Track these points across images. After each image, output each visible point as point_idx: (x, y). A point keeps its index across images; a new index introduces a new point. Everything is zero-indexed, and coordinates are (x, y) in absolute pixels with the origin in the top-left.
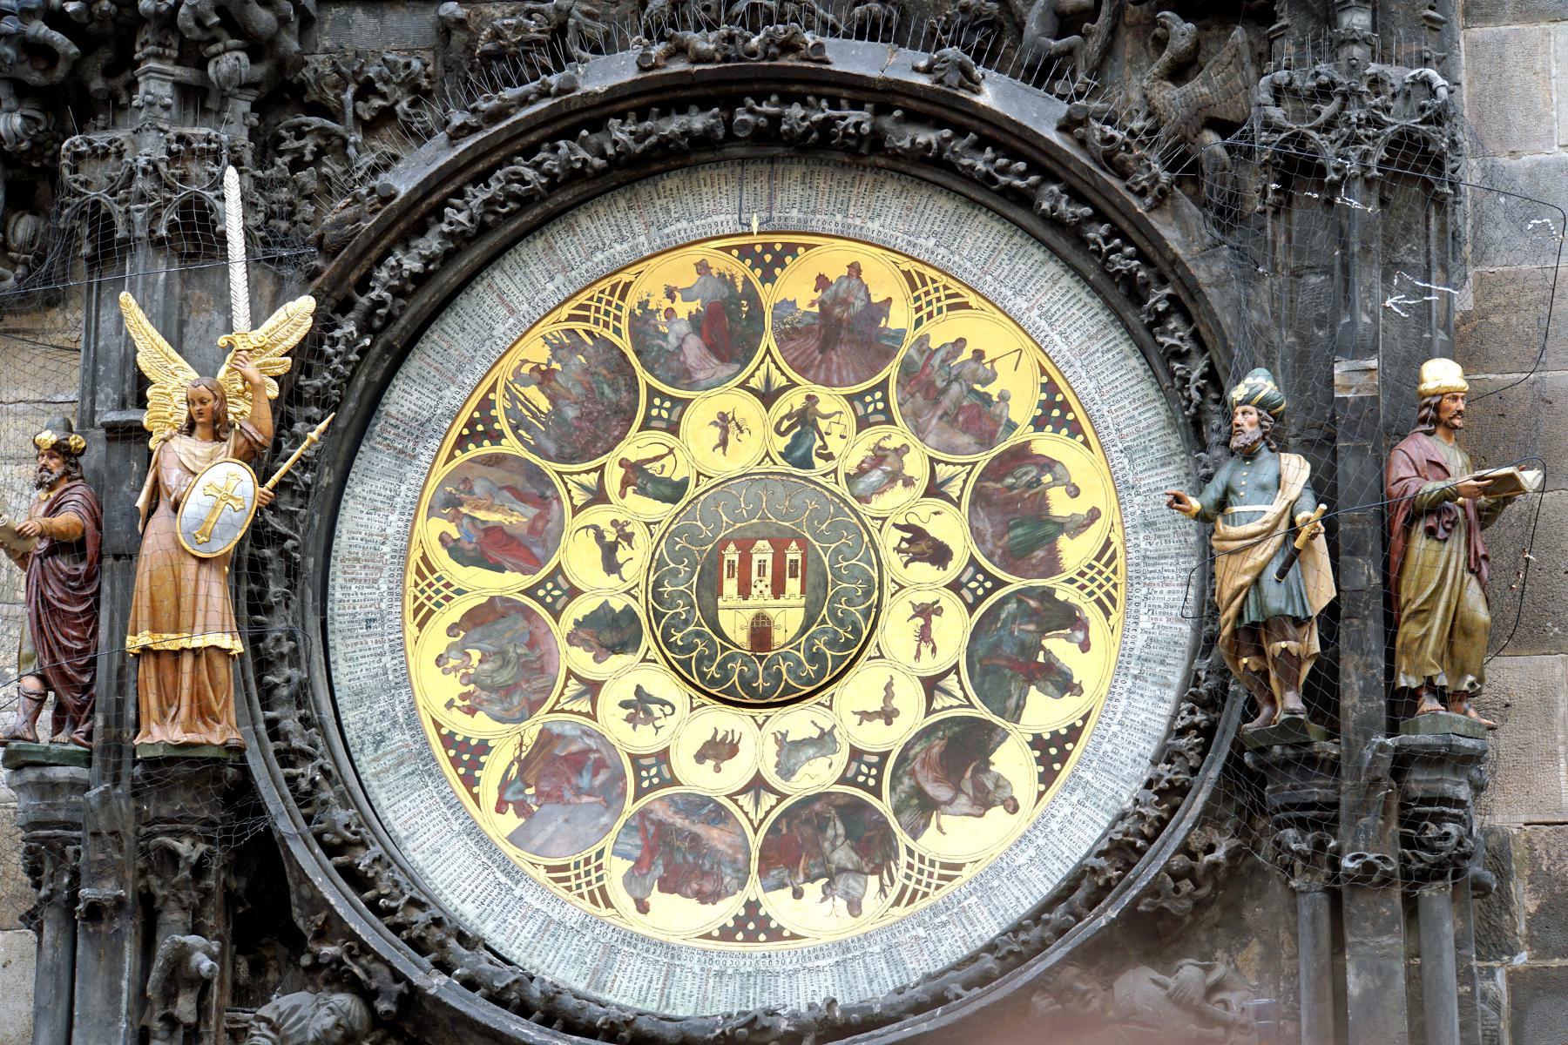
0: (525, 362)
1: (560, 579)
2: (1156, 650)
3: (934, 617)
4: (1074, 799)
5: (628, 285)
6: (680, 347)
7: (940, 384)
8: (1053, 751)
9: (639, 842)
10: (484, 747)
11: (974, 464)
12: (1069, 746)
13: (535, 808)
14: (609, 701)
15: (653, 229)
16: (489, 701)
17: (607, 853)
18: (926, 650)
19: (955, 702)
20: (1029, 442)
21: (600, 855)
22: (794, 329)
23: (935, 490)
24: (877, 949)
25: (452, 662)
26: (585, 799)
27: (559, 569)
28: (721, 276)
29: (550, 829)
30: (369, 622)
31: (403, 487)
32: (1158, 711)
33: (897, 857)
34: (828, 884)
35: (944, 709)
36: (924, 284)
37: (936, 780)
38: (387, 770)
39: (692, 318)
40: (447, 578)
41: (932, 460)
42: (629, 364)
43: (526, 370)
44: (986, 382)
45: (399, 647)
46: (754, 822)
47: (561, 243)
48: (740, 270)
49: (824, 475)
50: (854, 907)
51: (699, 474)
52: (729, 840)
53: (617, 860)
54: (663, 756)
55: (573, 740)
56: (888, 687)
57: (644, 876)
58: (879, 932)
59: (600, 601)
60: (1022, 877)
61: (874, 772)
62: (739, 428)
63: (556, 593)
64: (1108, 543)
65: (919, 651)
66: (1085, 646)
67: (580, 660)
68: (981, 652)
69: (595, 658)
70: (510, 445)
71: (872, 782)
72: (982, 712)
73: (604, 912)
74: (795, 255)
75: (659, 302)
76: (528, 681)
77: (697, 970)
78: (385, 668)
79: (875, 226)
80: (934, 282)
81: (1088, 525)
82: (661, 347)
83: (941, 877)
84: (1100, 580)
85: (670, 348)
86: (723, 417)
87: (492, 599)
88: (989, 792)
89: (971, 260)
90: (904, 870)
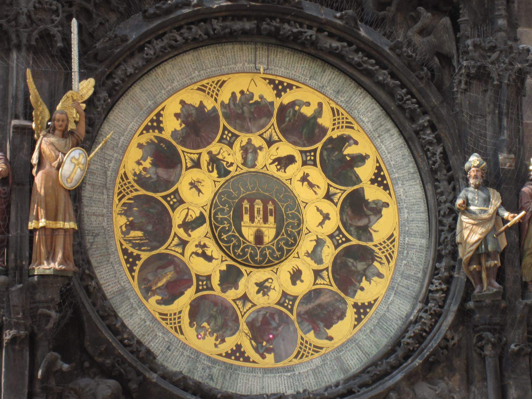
0: (121, 227)
1: (201, 278)
2: (376, 124)
3: (308, 178)
5: (125, 173)
6: (158, 176)
7: (240, 112)
9: (307, 324)
10: (239, 347)
12: (382, 173)
13: (271, 346)
15: (115, 149)
16: (224, 332)
17: (303, 336)
18: (316, 189)
19: (340, 194)
20: (281, 103)
21: (302, 338)
22: (183, 137)
23: (270, 143)
24: (400, 279)
25: (202, 333)
26: (280, 329)
27: (197, 276)
28: (147, 143)
29: (282, 347)
30: (168, 348)
31: (132, 300)
32: (394, 140)
33: (374, 251)
34: (366, 278)
35: (339, 199)
36: (206, 87)
37: (359, 220)
38: (223, 383)
39: (153, 164)
40: (173, 313)
41: (261, 135)
43: (124, 229)
45: (185, 346)
46: (328, 283)
48: (150, 136)
49: (236, 171)
50: (380, 275)
51: (202, 207)
52: (328, 296)
53: (308, 335)
54: (284, 294)
56: (318, 210)
57: (320, 331)
58: (394, 273)
60: (411, 219)
61: (341, 236)
62: (199, 182)
63: (205, 283)
64: (332, 109)
66: (356, 143)
67: (231, 295)
70: (145, 256)
71: (344, 239)
72: (350, 189)
73: (323, 352)
75: (138, 169)
76: (227, 316)
77: (365, 337)
78: (188, 356)
79: (176, 84)
80: (208, 84)
82: (153, 182)
84: (341, 121)
85: (155, 179)
86: (191, 184)
87: (191, 304)
88: (376, 208)
89: (213, 67)
90: (380, 252)
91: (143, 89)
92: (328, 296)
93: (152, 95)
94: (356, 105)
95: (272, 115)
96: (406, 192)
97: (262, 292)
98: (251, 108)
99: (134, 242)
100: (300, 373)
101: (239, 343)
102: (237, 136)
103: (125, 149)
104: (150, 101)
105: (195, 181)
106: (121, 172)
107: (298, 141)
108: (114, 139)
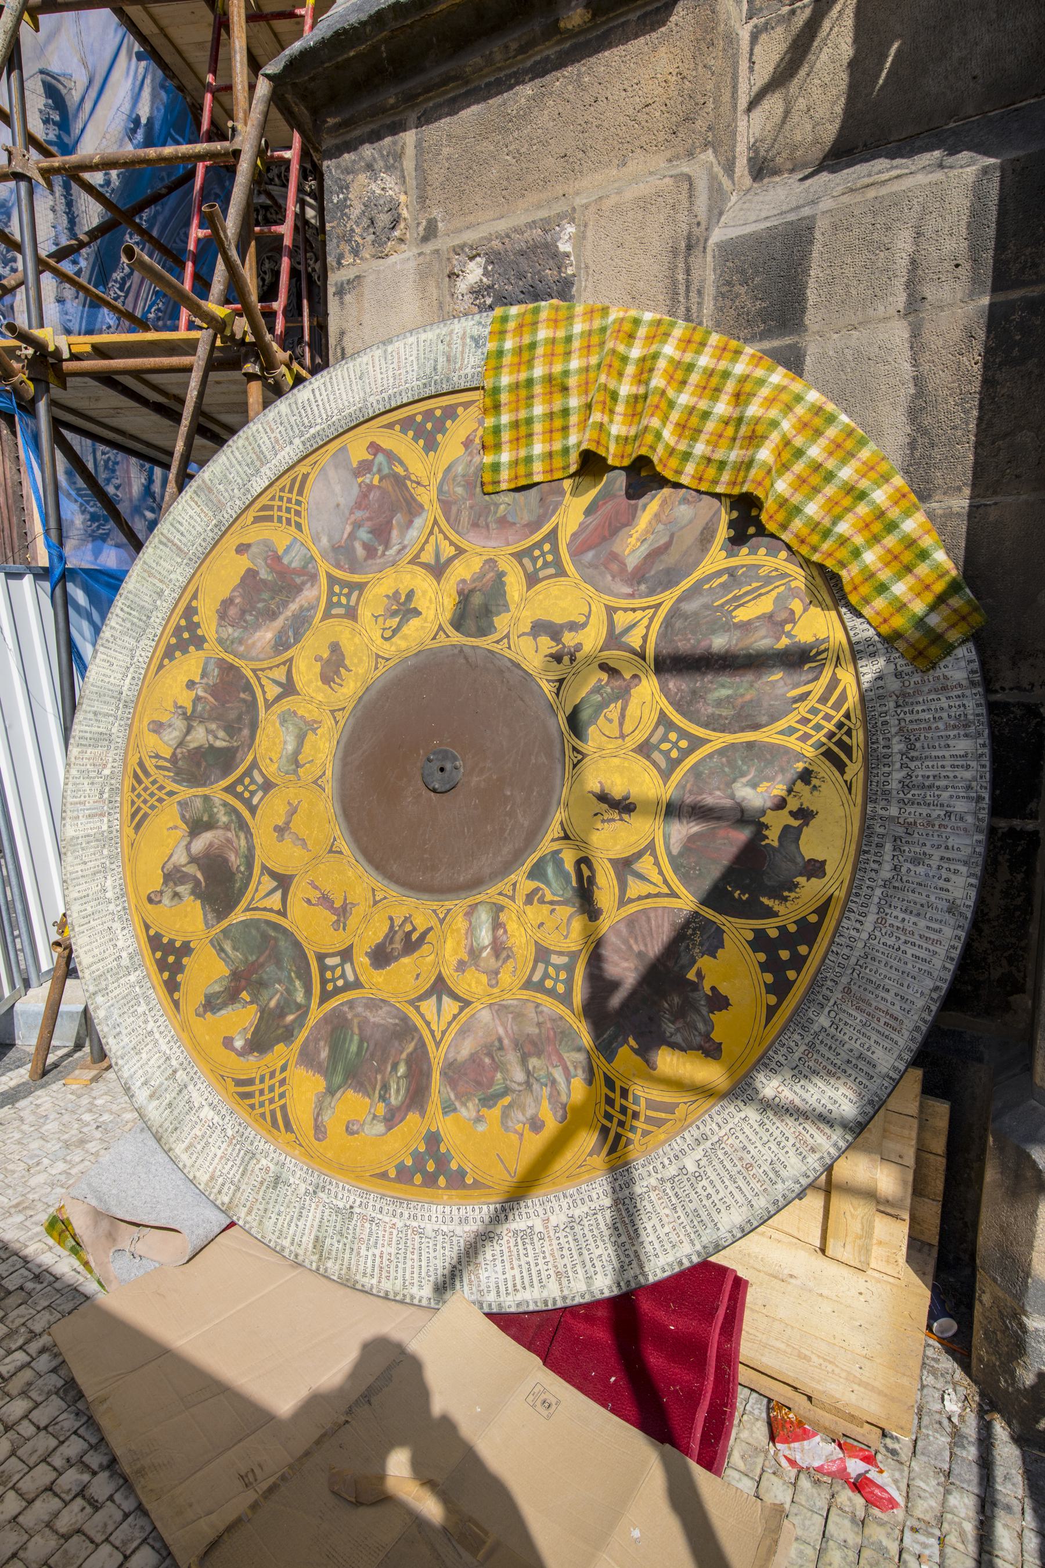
1: (551, 571)
3: (335, 918)
4: (124, 954)
5: (841, 767)
7: (533, 1062)
8: (171, 959)
9: (294, 565)
10: (431, 446)
11: (438, 1044)
13: (360, 480)
14: (422, 583)
15: (900, 831)
18: (314, 895)
19: (257, 897)
21: (299, 526)
24: (114, 730)
26: (348, 529)
27: (562, 573)
28: (793, 887)
29: (338, 489)
32: (140, 1072)
33: (174, 781)
34: (185, 714)
37: (211, 845)
42: (742, 730)
47: (944, 703)
48: (787, 913)
50: (157, 727)
52: (259, 644)
54: (352, 614)
55: (402, 535)
57: (265, 560)
59: (512, 607)
60: (98, 876)
61: (247, 795)
65: (316, 888)
68: (282, 944)
69: (464, 581)
72: (238, 916)
74: (770, 989)
76: (471, 507)
77: (173, 576)
81: (316, 1120)
82: (743, 775)
83: (139, 809)
85: (737, 785)
88: (176, 885)
90: (161, 781)
91: (861, 1064)
92: (259, 644)
93: (823, 1050)
94: (230, 1150)
95: (444, 1073)
96: (111, 940)
97: (402, 600)
98: (504, 1079)
99: (754, 585)
100: (291, 443)
101: (432, 453)
102: (528, 985)
103: (867, 839)
104: (823, 1029)
105: (622, 820)
106: (855, 768)
107: (368, 1014)
108: (916, 861)
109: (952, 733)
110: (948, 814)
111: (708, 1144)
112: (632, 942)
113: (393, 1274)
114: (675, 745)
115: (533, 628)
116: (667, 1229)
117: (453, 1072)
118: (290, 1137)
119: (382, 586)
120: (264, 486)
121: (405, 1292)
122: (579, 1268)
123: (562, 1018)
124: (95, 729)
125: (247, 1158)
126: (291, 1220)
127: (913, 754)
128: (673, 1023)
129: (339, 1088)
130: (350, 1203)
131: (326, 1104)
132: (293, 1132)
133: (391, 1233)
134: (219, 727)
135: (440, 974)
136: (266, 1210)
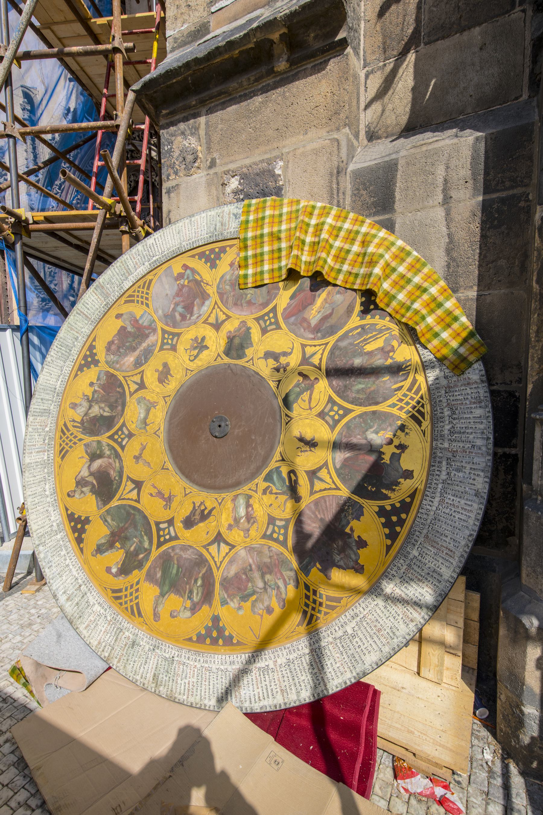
1: (274, 327)
3: (165, 503)
4: (55, 524)
5: (419, 423)
7: (268, 577)
9: (145, 324)
10: (213, 266)
11: (218, 569)
13: (178, 282)
14: (209, 333)
15: (450, 455)
19: (125, 493)
21: (147, 305)
24: (52, 408)
26: (172, 306)
27: (279, 327)
28: (398, 484)
29: (167, 287)
32: (62, 586)
33: (82, 433)
34: (88, 399)
37: (101, 466)
42: (370, 405)
44: (253, 606)
48: (395, 497)
49: (257, 485)
50: (74, 406)
52: (127, 364)
54: (174, 348)
55: (199, 309)
57: (130, 322)
59: (254, 345)
60: (42, 483)
61: (120, 440)
65: (155, 487)
68: (137, 517)
69: (230, 332)
72: (115, 503)
74: (388, 536)
77: (83, 330)
81: (154, 610)
82: (371, 428)
83: (64, 448)
85: (368, 433)
88: (82, 487)
90: (75, 434)
91: (435, 575)
93: (415, 568)
94: (109, 627)
95: (221, 584)
96: (48, 517)
97: (199, 341)
98: (253, 586)
99: (374, 333)
101: (214, 269)
102: (264, 536)
103: (433, 459)
105: (311, 450)
106: (426, 424)
107: (182, 553)
108: (458, 470)
109: (473, 406)
110: (473, 446)
111: (358, 618)
112: (317, 513)
113: (195, 693)
114: (337, 412)
115: (265, 355)
116: (338, 665)
117: (226, 583)
118: (141, 620)
119: (189, 335)
120: (130, 285)
121: (202, 703)
122: (293, 687)
123: (282, 553)
124: (42, 407)
125: (118, 632)
126: (141, 665)
127: (454, 416)
128: (339, 555)
129: (167, 593)
130: (172, 655)
131: (160, 601)
132: (142, 617)
133: (194, 671)
134: (106, 405)
135: (219, 532)
136: (128, 660)
